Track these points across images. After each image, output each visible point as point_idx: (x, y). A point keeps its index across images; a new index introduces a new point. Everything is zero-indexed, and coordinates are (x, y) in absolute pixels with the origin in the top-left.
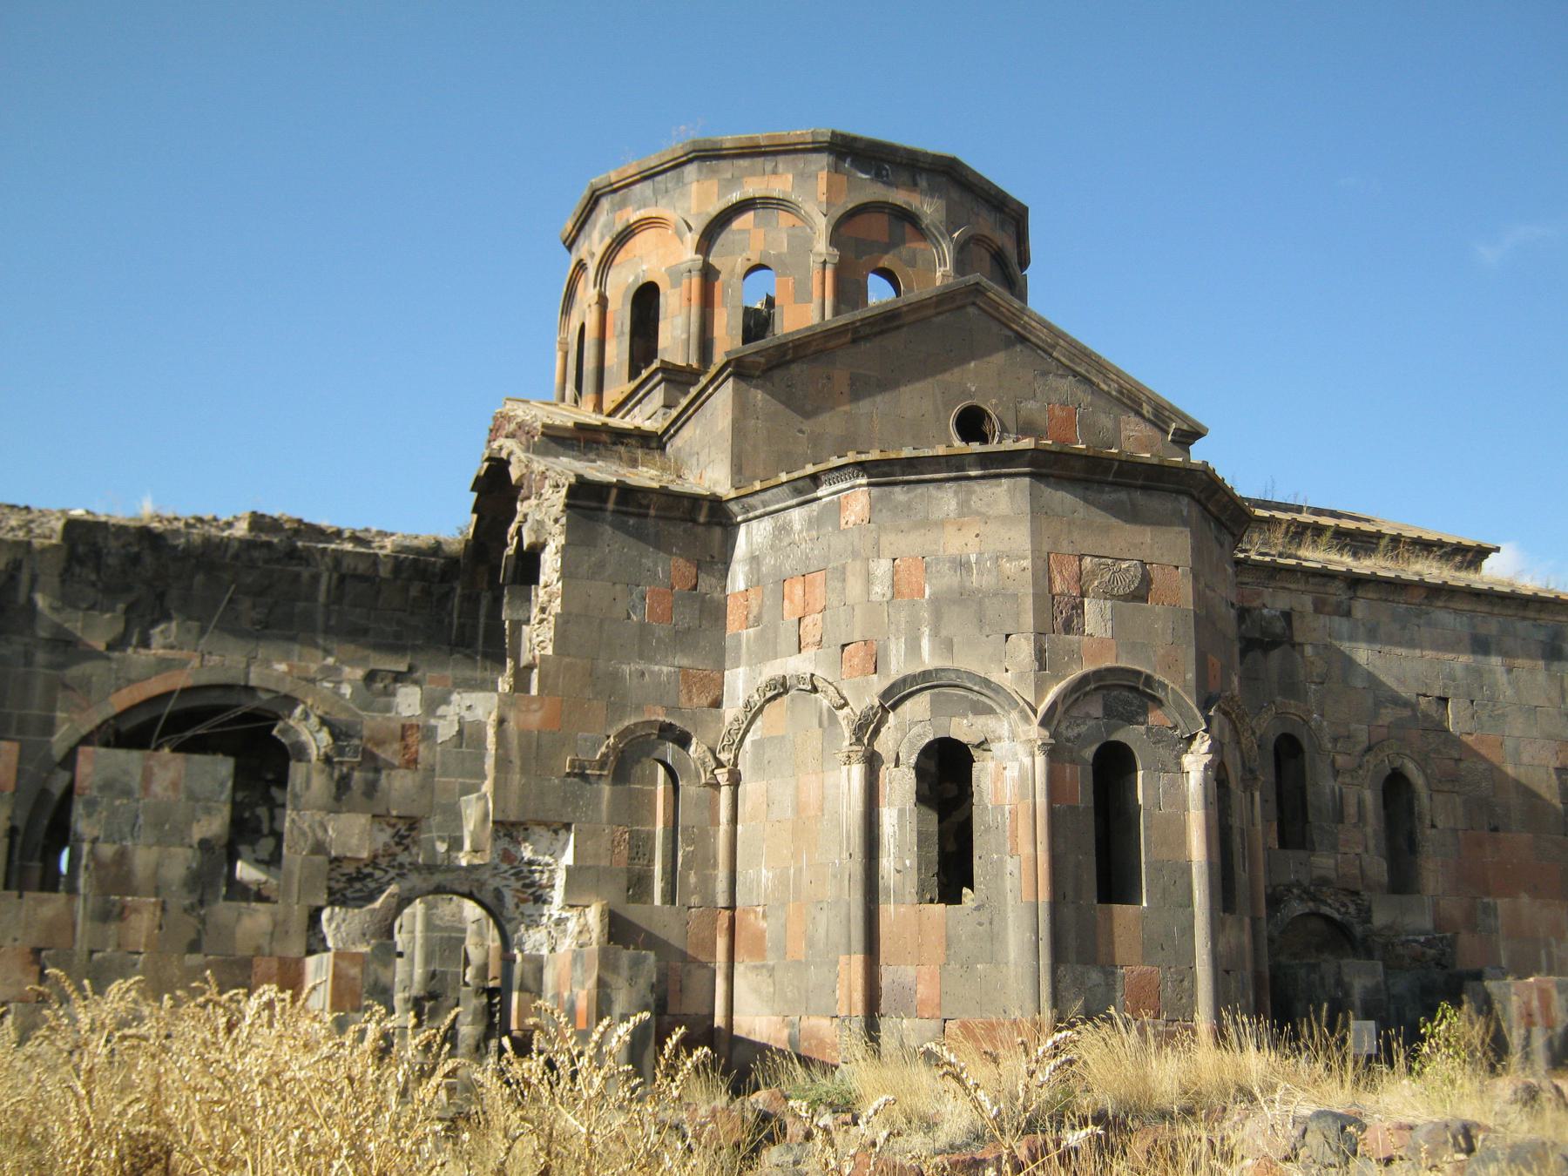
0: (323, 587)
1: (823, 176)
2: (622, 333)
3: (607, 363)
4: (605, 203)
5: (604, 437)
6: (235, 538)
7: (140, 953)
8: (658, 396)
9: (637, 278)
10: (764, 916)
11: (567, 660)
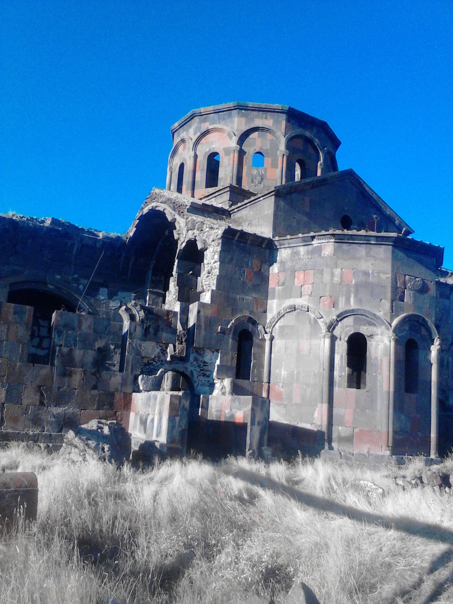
0: (75, 249)
1: (284, 122)
2: (203, 169)
3: (196, 180)
4: (197, 119)
5: (210, 210)
6: (46, 227)
7: (76, 389)
8: (226, 196)
9: (210, 149)
10: (282, 387)
11: (220, 292)
